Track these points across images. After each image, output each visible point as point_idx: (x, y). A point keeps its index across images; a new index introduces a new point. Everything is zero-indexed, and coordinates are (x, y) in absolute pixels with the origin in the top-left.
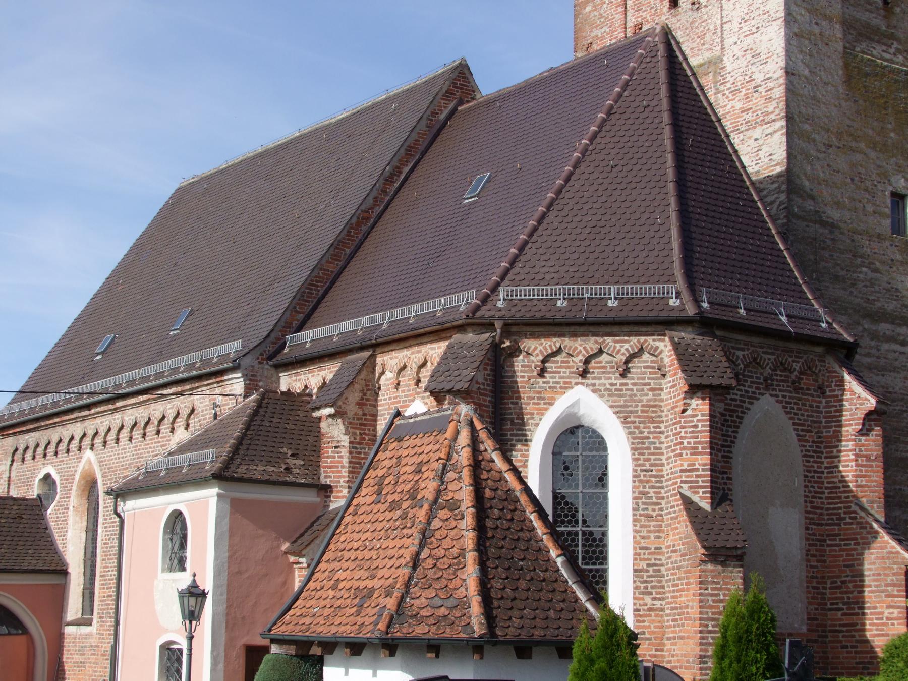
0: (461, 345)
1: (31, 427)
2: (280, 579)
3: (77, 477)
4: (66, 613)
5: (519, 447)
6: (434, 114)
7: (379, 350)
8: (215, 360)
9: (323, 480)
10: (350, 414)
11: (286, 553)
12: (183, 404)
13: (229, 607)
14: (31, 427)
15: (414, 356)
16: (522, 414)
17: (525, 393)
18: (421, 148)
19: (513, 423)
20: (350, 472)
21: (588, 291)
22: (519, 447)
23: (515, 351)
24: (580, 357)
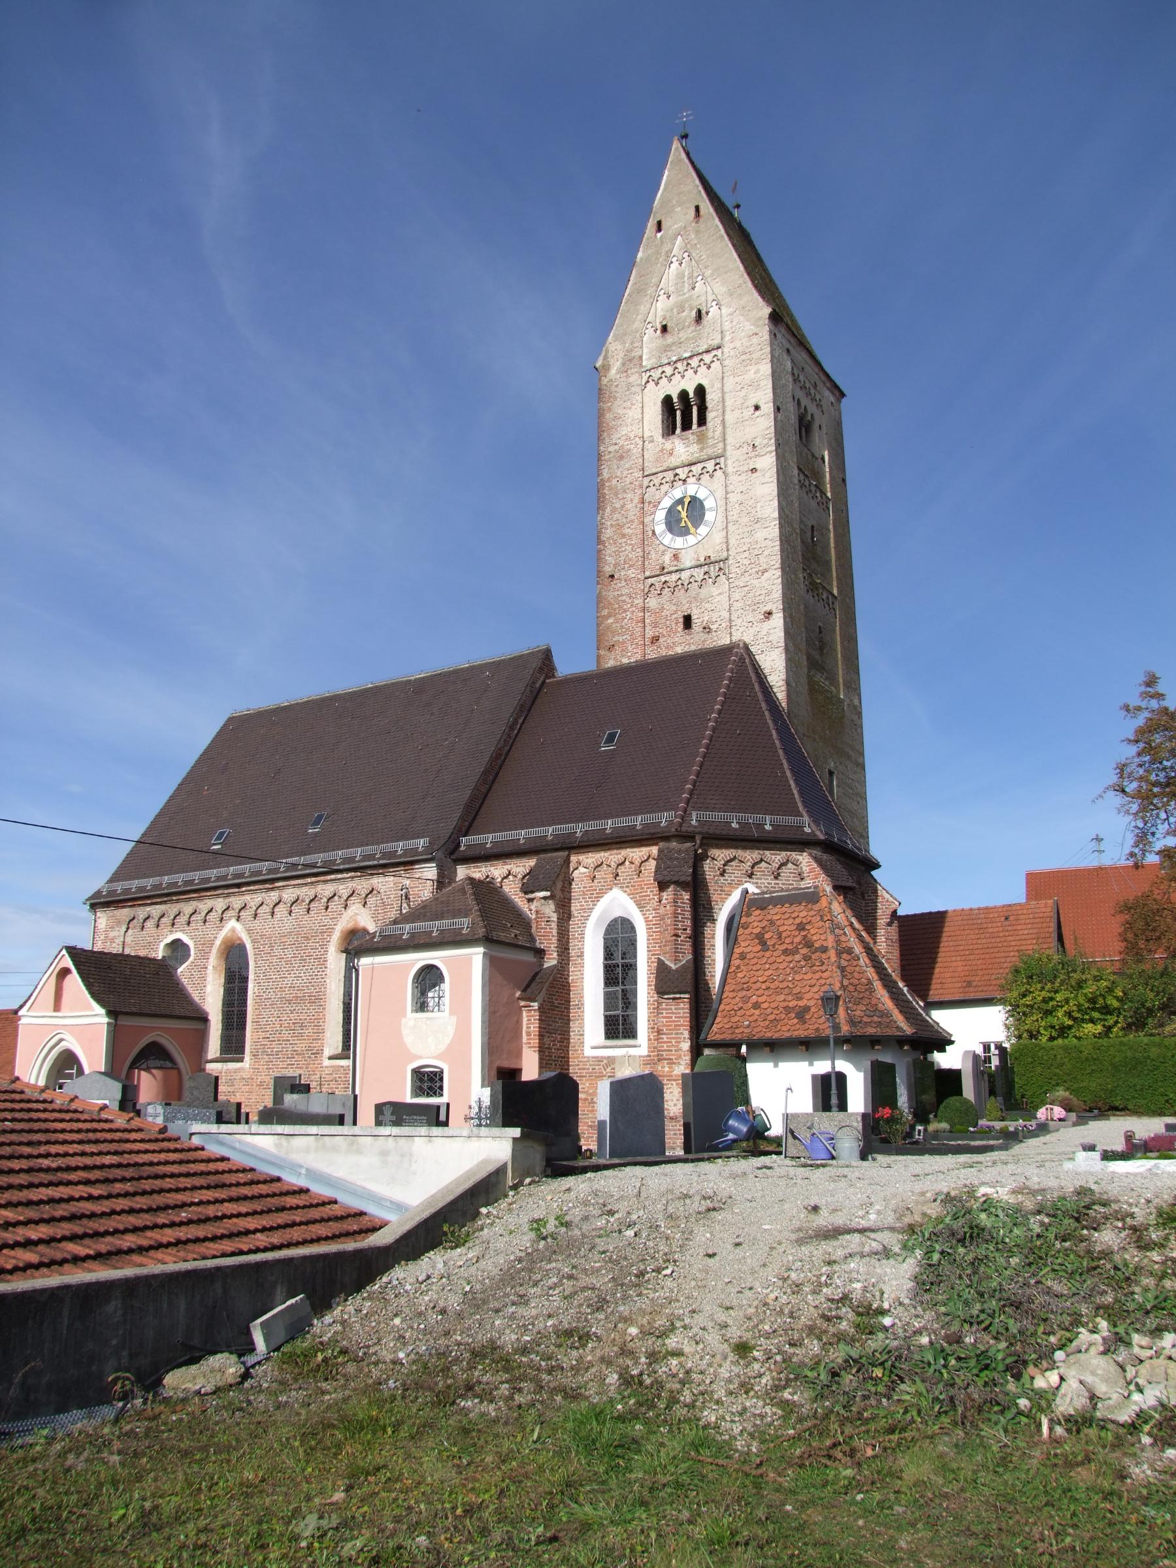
0: (670, 850)
1: (158, 900)
2: (515, 1019)
3: (218, 942)
4: (206, 1052)
5: (709, 924)
6: (534, 683)
7: (572, 851)
8: (400, 852)
9: (538, 945)
10: (558, 897)
11: (519, 999)
12: (362, 884)
13: (489, 1038)
14: (158, 900)
16: (710, 901)
17: (712, 888)
18: (528, 706)
19: (704, 908)
20: (558, 940)
21: (751, 818)
22: (709, 924)
23: (704, 857)
24: (749, 864)
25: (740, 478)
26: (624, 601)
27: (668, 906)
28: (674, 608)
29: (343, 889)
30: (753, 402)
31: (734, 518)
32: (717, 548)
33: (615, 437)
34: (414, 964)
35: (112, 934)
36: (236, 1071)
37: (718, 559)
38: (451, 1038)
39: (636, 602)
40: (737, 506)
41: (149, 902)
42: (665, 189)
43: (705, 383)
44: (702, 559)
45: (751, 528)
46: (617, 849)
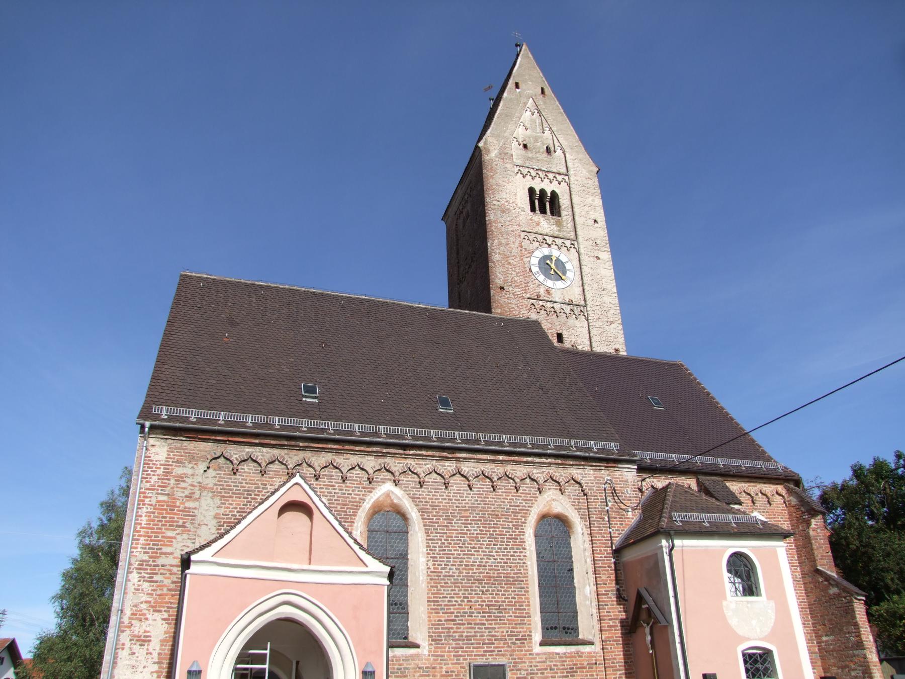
1: (273, 442)
3: (367, 505)
14: (273, 442)
15: (751, 488)
25: (589, 259)
26: (513, 308)
27: (819, 530)
28: (550, 326)
29: (540, 473)
30: (594, 217)
31: (589, 282)
32: (577, 296)
33: (498, 197)
34: (725, 551)
35: (179, 471)
36: (407, 659)
37: (578, 303)
38: (773, 621)
39: (523, 312)
40: (589, 275)
41: (257, 441)
42: (519, 67)
43: (557, 191)
44: (567, 301)
45: (599, 293)
46: (753, 482)
